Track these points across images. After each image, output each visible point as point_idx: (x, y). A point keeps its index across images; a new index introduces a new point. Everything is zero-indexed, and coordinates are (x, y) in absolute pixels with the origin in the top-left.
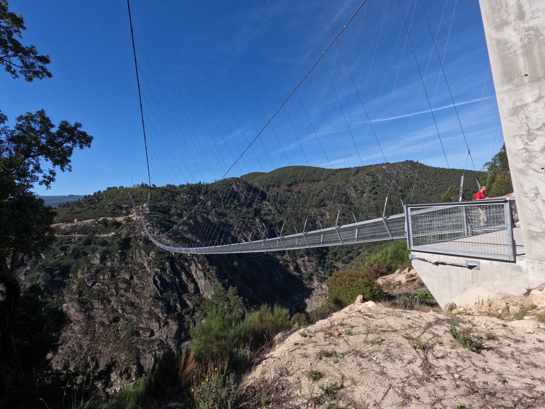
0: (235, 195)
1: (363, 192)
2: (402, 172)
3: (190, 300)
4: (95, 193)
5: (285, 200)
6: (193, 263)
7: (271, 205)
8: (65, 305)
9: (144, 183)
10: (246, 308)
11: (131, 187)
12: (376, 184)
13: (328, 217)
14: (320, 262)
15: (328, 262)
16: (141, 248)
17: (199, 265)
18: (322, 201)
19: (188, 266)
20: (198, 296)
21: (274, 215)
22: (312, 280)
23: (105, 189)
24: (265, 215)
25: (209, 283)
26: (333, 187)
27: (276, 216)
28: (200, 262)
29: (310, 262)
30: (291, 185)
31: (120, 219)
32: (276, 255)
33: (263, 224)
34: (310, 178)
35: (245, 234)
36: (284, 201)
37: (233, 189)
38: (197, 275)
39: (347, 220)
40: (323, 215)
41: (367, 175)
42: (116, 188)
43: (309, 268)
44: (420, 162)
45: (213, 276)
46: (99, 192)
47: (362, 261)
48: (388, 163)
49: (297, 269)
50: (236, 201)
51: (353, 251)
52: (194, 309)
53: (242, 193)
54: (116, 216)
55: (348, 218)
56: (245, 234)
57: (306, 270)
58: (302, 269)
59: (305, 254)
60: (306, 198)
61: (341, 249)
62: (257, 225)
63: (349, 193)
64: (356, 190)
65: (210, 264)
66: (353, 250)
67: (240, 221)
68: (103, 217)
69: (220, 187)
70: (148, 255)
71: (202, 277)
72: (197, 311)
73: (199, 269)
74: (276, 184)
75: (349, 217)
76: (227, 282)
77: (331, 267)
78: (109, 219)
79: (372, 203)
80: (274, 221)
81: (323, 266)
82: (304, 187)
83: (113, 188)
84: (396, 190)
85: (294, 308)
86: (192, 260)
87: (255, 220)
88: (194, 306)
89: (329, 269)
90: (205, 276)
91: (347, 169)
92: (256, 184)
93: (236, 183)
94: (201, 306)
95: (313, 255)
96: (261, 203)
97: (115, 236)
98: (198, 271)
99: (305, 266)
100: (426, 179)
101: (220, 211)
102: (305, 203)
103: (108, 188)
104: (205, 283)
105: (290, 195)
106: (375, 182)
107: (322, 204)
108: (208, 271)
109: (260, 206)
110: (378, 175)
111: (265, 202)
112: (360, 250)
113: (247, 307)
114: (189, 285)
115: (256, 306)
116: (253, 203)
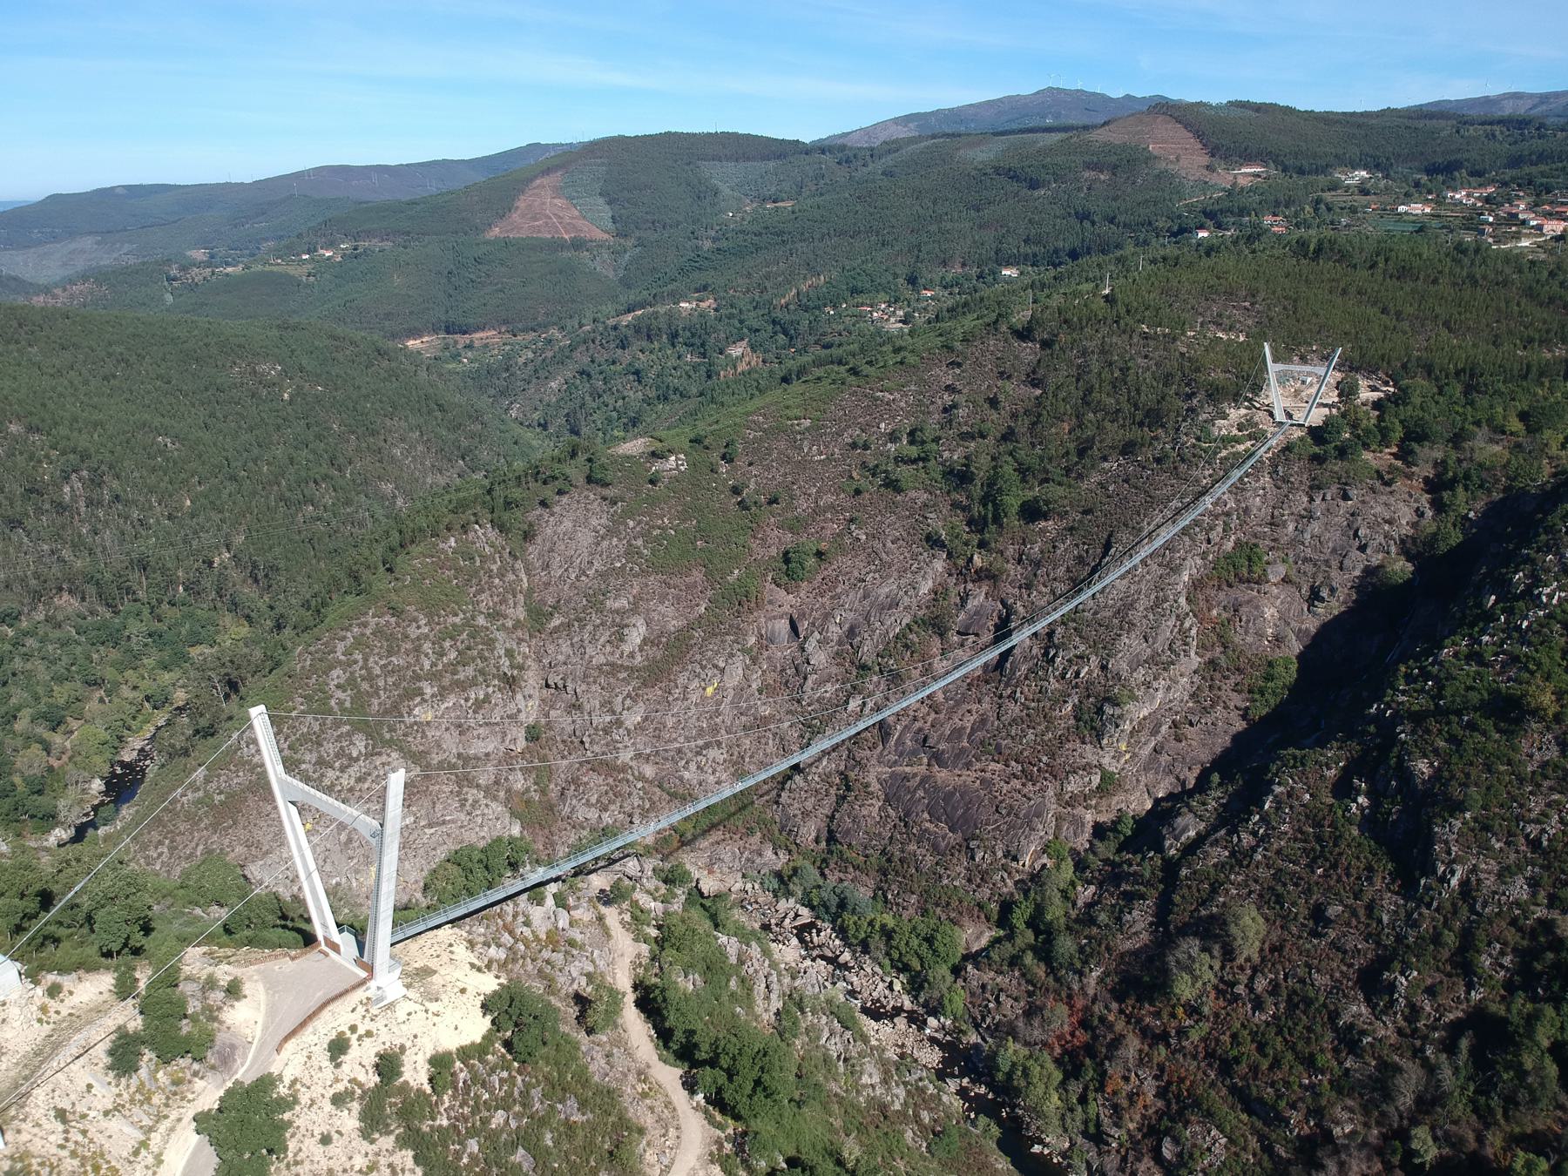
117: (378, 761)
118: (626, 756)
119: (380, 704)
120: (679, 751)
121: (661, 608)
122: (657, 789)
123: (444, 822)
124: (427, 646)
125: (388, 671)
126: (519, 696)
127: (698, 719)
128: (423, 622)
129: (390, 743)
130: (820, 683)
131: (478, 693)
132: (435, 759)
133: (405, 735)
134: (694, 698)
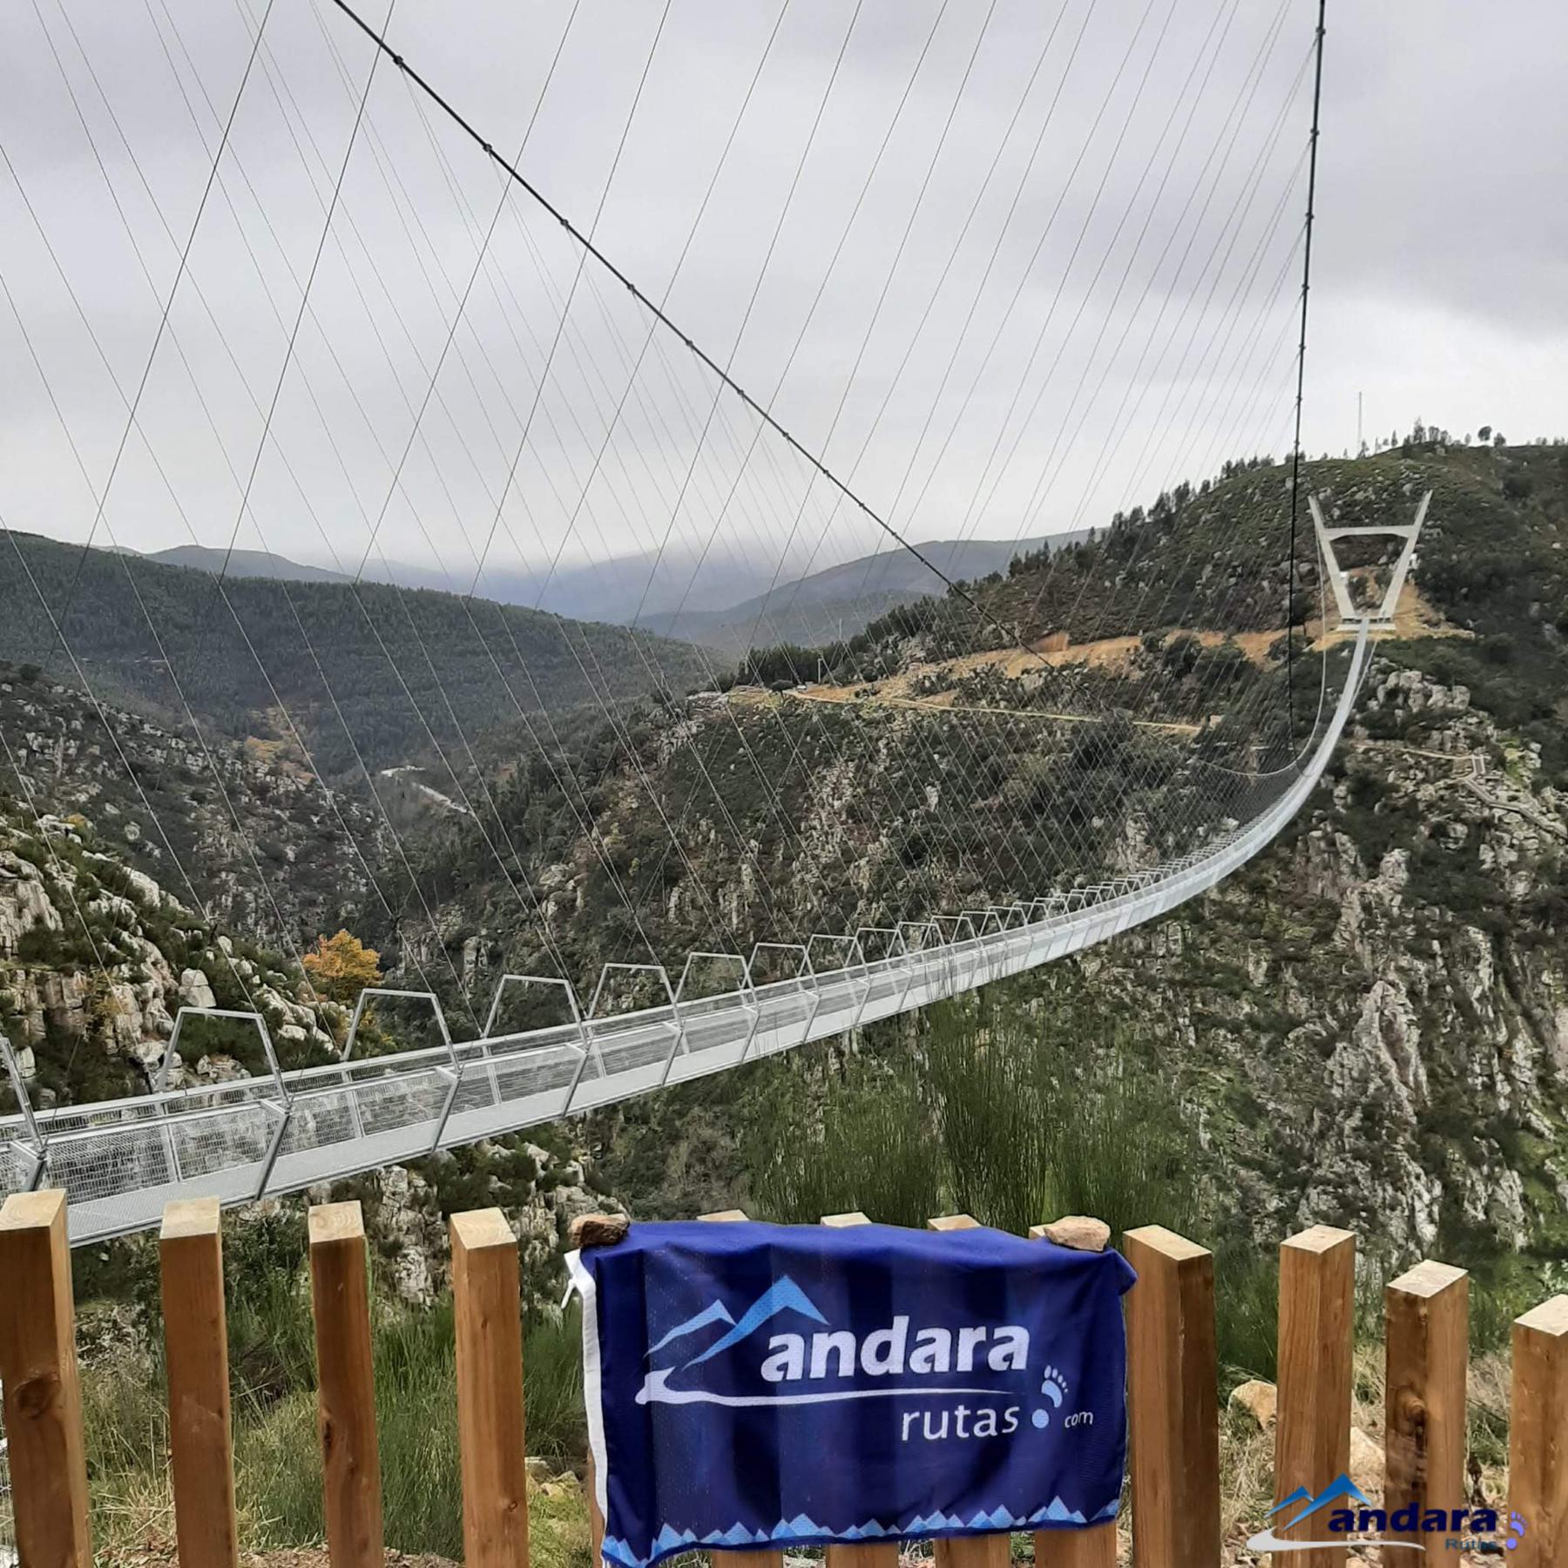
4: (1161, 504)
8: (984, 1036)
9: (1426, 426)
11: (1353, 456)
16: (1336, 819)
23: (1214, 474)
31: (1256, 646)
42: (1267, 462)
46: (1183, 492)
54: (1240, 629)
68: (1184, 626)
70: (1373, 865)
78: (1210, 640)
83: (1254, 463)
97: (1217, 735)
103: (1229, 469)
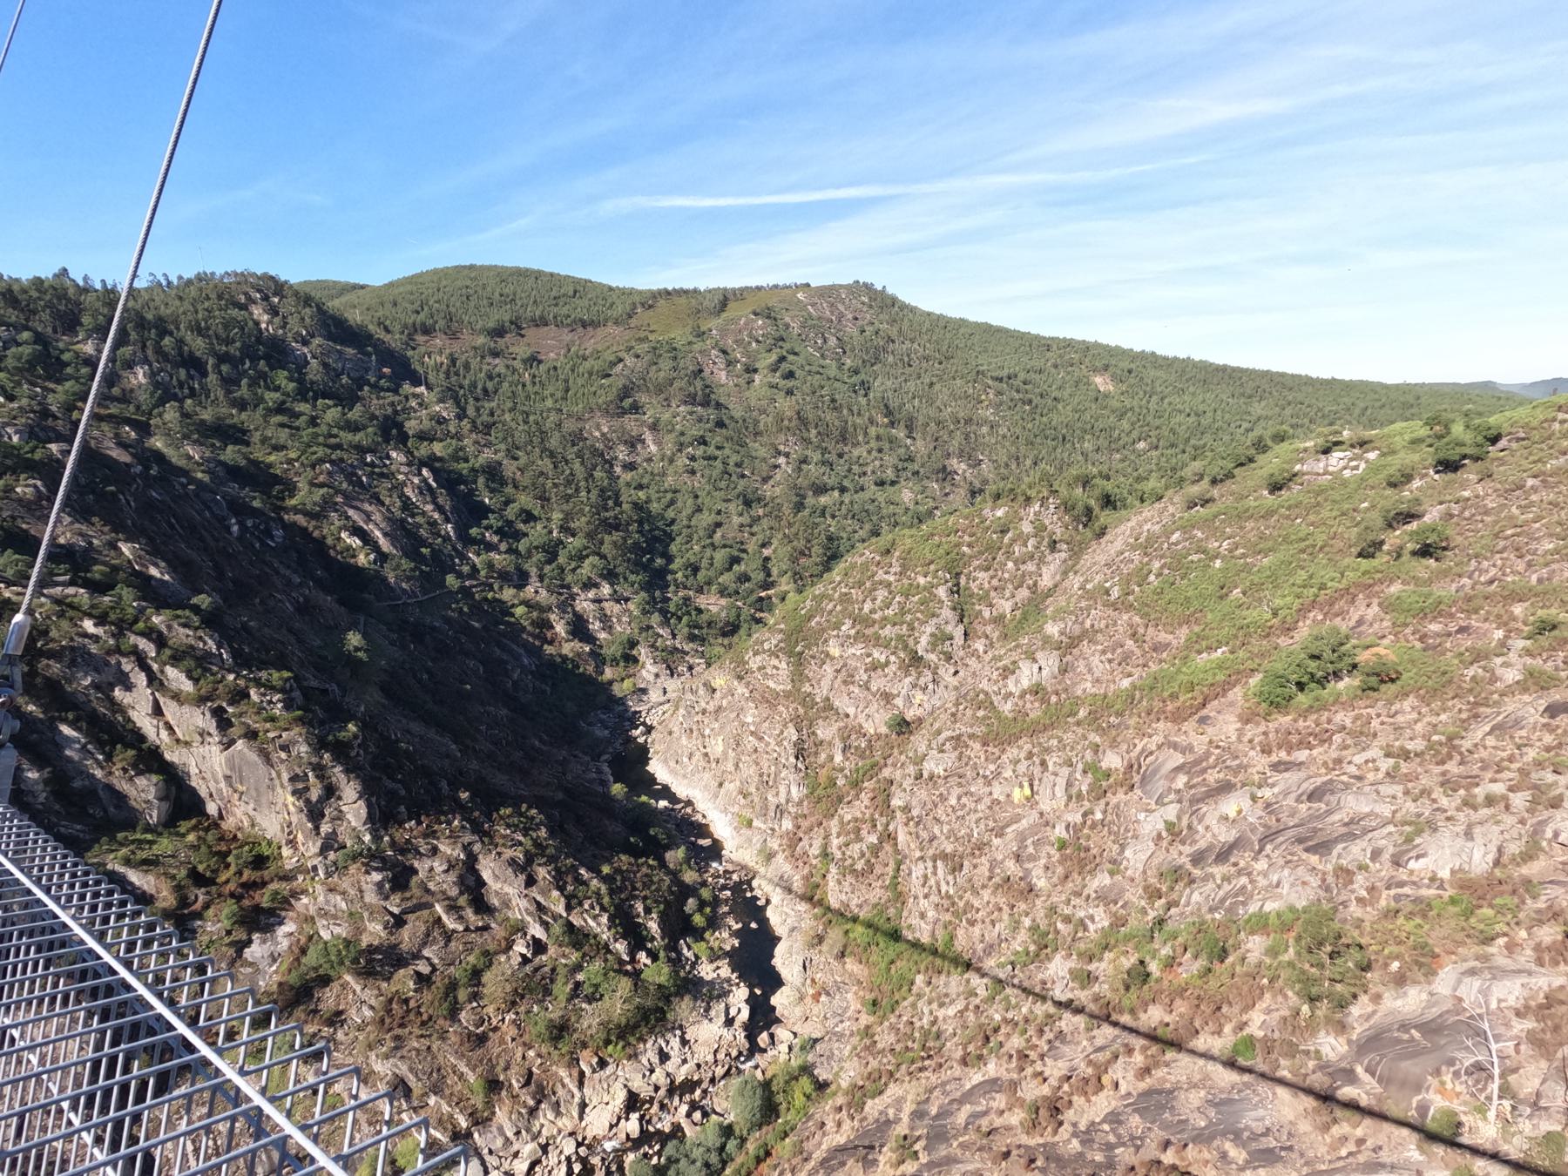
0: (276, 352)
1: (751, 370)
2: (850, 316)
3: (148, 864)
5: (490, 385)
6: (127, 665)
7: (441, 401)
10: (473, 832)
12: (787, 346)
13: (653, 448)
14: (653, 601)
15: (675, 597)
17: (171, 672)
18: (626, 396)
19: (96, 686)
20: (195, 828)
21: (458, 436)
22: (636, 661)
24: (423, 436)
25: (253, 757)
26: (655, 349)
27: (466, 442)
28: (176, 659)
29: (618, 601)
30: (499, 332)
32: (496, 587)
33: (425, 472)
34: (565, 310)
35: (351, 512)
36: (485, 390)
37: (257, 323)
38: (169, 728)
39: (716, 458)
40: (633, 443)
41: (756, 314)
43: (619, 621)
44: (890, 291)
45: (273, 719)
47: (860, 584)
48: (808, 285)
49: (579, 629)
50: (281, 377)
51: (744, 555)
52: (184, 902)
53: (305, 343)
55: (718, 453)
56: (351, 512)
57: (608, 627)
58: (595, 626)
59: (602, 576)
60: (566, 381)
61: (708, 552)
62: (400, 477)
63: (707, 371)
64: (729, 364)
65: (242, 661)
66: (744, 551)
67: (322, 461)
69: (187, 306)
71: (203, 734)
72: (207, 906)
73: (177, 697)
74: (441, 324)
75: (718, 448)
76: (355, 737)
77: (689, 613)
79: (786, 405)
80: (466, 460)
81: (664, 613)
82: (551, 344)
84: (839, 368)
85: (606, 768)
86: (118, 650)
87: (388, 457)
88: (178, 888)
89: (685, 619)
90: (224, 723)
91: (686, 292)
92: (355, 317)
93: (266, 298)
94: (222, 878)
95: (626, 579)
96: (396, 391)
98: (170, 708)
99: (605, 619)
100: (912, 341)
101: (207, 415)
102: (564, 399)
104: (231, 763)
105: (501, 369)
106: (782, 339)
107: (625, 403)
108: (240, 696)
109: (392, 404)
110: (787, 319)
111: (407, 388)
112: (766, 552)
113: (477, 829)
114: (123, 786)
115: (508, 811)
116: (361, 389)
117: (775, 662)
118: (896, 802)
119: (818, 623)
120: (932, 839)
121: (1095, 661)
122: (892, 865)
123: (761, 739)
124: (881, 594)
125: (845, 599)
126: (908, 680)
127: (978, 821)
128: (893, 570)
129: (790, 654)
130: (1104, 898)
131: (879, 655)
132: (807, 688)
133: (813, 657)
134: (998, 791)
